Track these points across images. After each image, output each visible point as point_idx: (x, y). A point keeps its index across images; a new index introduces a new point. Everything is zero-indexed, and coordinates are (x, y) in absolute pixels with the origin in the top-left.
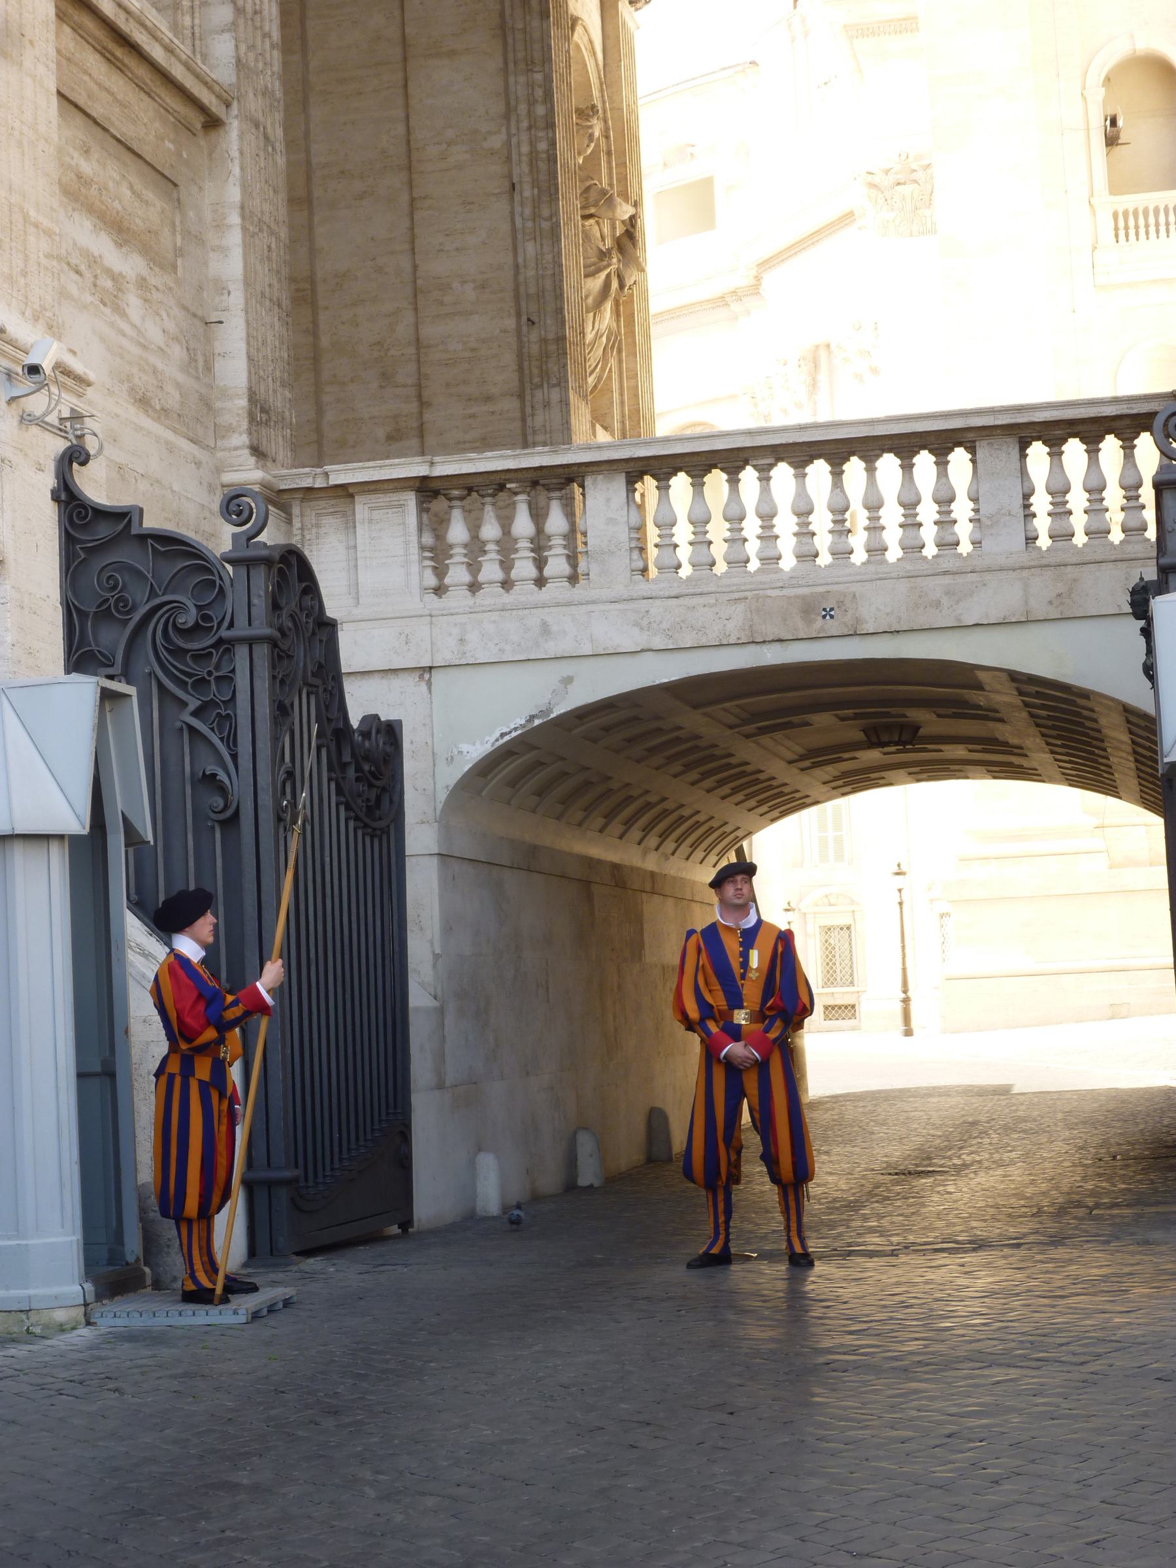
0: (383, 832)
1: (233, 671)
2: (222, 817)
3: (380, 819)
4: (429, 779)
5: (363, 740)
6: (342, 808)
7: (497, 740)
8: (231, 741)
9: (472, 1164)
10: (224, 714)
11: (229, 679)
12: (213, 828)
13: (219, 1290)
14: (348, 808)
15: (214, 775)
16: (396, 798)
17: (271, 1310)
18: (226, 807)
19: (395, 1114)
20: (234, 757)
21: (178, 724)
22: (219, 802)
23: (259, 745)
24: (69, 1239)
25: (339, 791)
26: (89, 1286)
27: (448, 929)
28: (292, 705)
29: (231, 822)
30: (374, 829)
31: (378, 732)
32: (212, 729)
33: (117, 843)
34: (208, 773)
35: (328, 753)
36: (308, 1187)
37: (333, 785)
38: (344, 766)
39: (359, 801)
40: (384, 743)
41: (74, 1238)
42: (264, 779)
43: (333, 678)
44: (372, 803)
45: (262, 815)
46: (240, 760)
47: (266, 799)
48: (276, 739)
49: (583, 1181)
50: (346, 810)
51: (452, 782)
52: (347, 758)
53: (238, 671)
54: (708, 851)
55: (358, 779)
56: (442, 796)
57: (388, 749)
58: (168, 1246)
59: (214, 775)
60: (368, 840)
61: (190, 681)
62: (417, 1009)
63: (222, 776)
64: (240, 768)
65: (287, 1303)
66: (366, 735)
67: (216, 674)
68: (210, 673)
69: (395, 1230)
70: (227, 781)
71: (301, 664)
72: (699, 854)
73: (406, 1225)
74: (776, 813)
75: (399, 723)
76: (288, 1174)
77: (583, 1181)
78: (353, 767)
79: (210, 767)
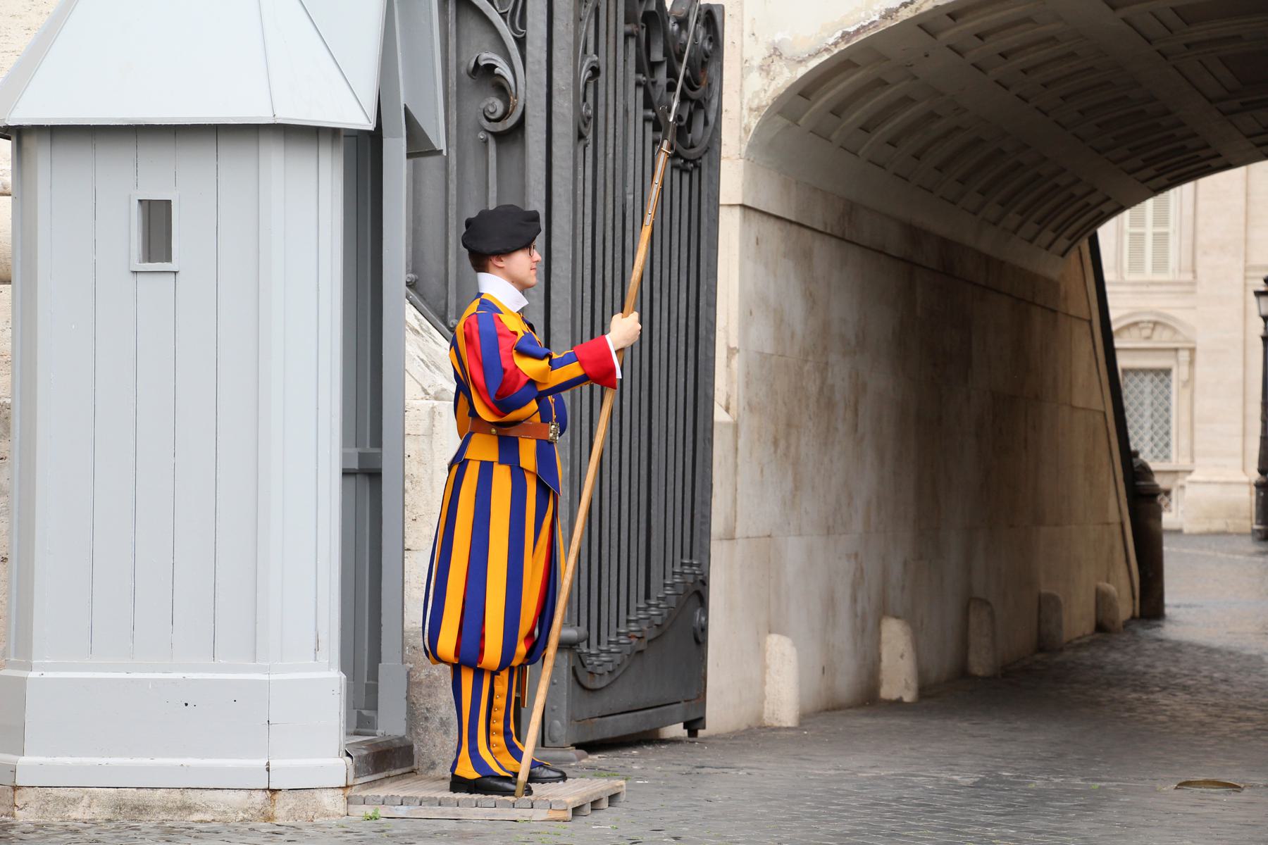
0: (696, 166)
2: (500, 127)
3: (692, 147)
4: (747, 92)
5: (680, 30)
6: (649, 127)
7: (836, 44)
9: (760, 649)
12: (486, 142)
13: (523, 777)
15: (491, 68)
16: (712, 117)
17: (595, 805)
19: (691, 565)
20: (521, 43)
22: (498, 106)
23: (558, 26)
27: (747, 315)
29: (512, 136)
30: (686, 161)
33: (395, 149)
34: (482, 63)
35: (638, 45)
36: (591, 655)
38: (654, 66)
40: (704, 38)
42: (562, 79)
44: (683, 124)
45: (557, 128)
46: (529, 47)
47: (564, 105)
48: (579, 19)
49: (889, 691)
50: (654, 130)
51: (766, 99)
52: (657, 55)
54: (1058, 231)
56: (754, 123)
57: (707, 46)
58: (426, 719)
59: (491, 68)
60: (676, 174)
62: (721, 423)
63: (503, 69)
64: (529, 59)
65: (613, 798)
69: (677, 730)
72: (1047, 236)
73: (693, 726)
74: (1163, 180)
75: (722, 8)
77: (889, 691)
79: (484, 55)
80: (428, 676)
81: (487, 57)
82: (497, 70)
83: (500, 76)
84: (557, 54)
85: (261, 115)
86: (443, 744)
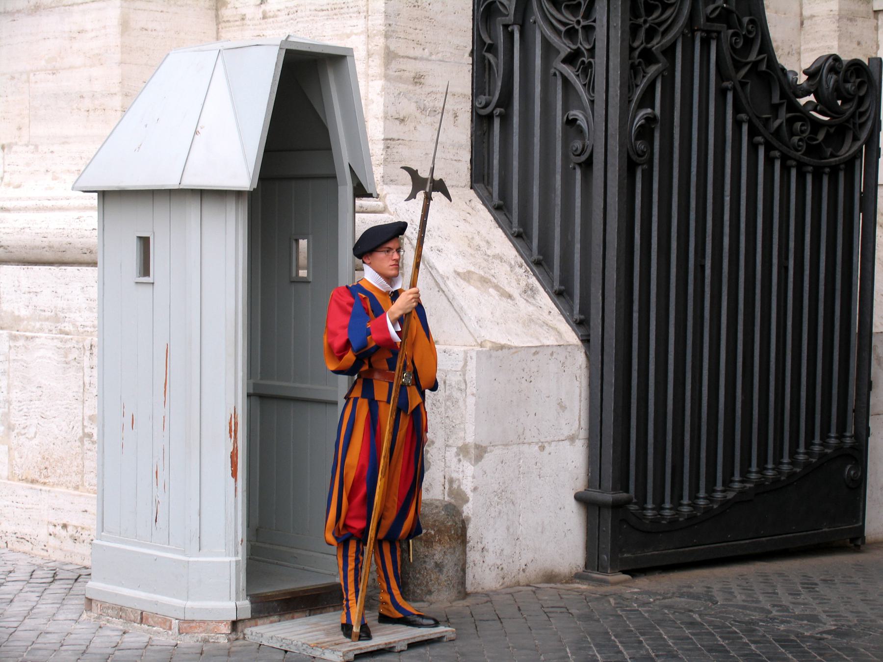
1: (594, 21)
8: (590, 86)
10: (586, 61)
11: (589, 30)
12: (574, 169)
14: (769, 148)
15: (575, 120)
18: (583, 151)
20: (592, 102)
21: (552, 71)
24: (227, 559)
25: (752, 133)
26: (246, 604)
28: (669, 52)
29: (587, 165)
31: (833, 70)
32: (578, 76)
34: (570, 118)
37: (745, 128)
39: (796, 139)
41: (234, 559)
43: (751, 22)
53: (597, 21)
55: (790, 122)
58: (425, 562)
59: (575, 120)
61: (563, 29)
63: (582, 122)
66: (812, 74)
67: (583, 23)
68: (578, 22)
70: (584, 125)
71: (686, 11)
73: (855, 541)
76: (608, 497)
78: (784, 108)
80: (426, 534)
81: (576, 113)
82: (578, 122)
83: (579, 126)
84: (610, 110)
85: (172, 182)
86: (438, 579)
